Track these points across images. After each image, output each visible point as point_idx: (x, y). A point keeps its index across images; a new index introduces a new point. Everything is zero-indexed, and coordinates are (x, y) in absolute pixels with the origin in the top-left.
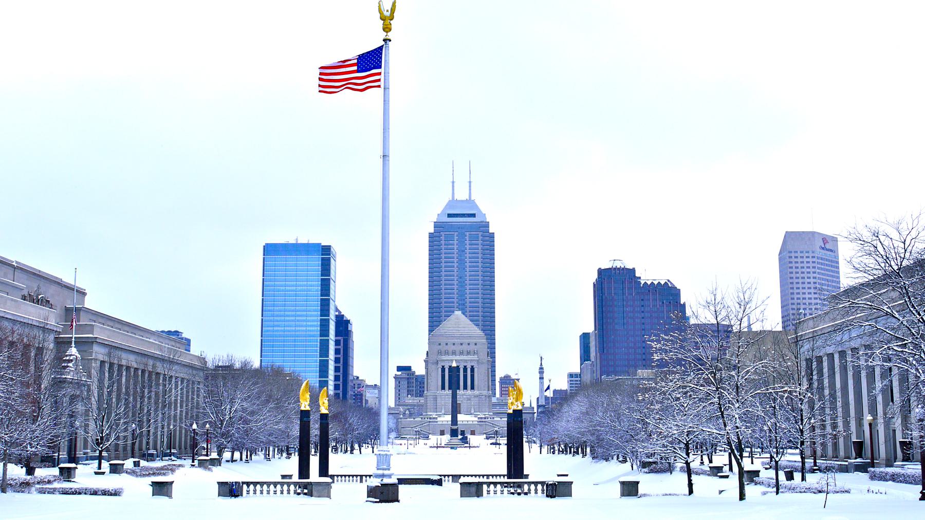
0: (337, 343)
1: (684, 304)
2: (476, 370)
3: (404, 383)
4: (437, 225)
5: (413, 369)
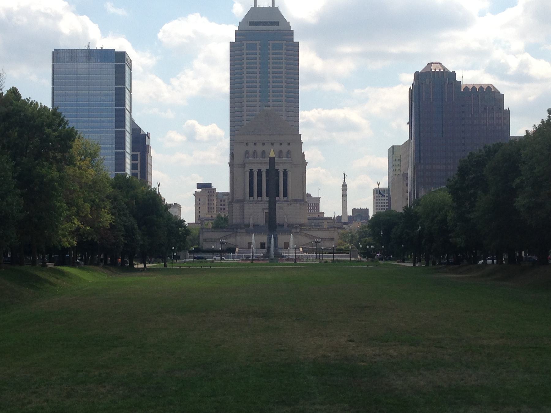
0: (134, 158)
1: (508, 111)
2: (289, 175)
3: (205, 200)
4: (237, 34)
5: (214, 186)
